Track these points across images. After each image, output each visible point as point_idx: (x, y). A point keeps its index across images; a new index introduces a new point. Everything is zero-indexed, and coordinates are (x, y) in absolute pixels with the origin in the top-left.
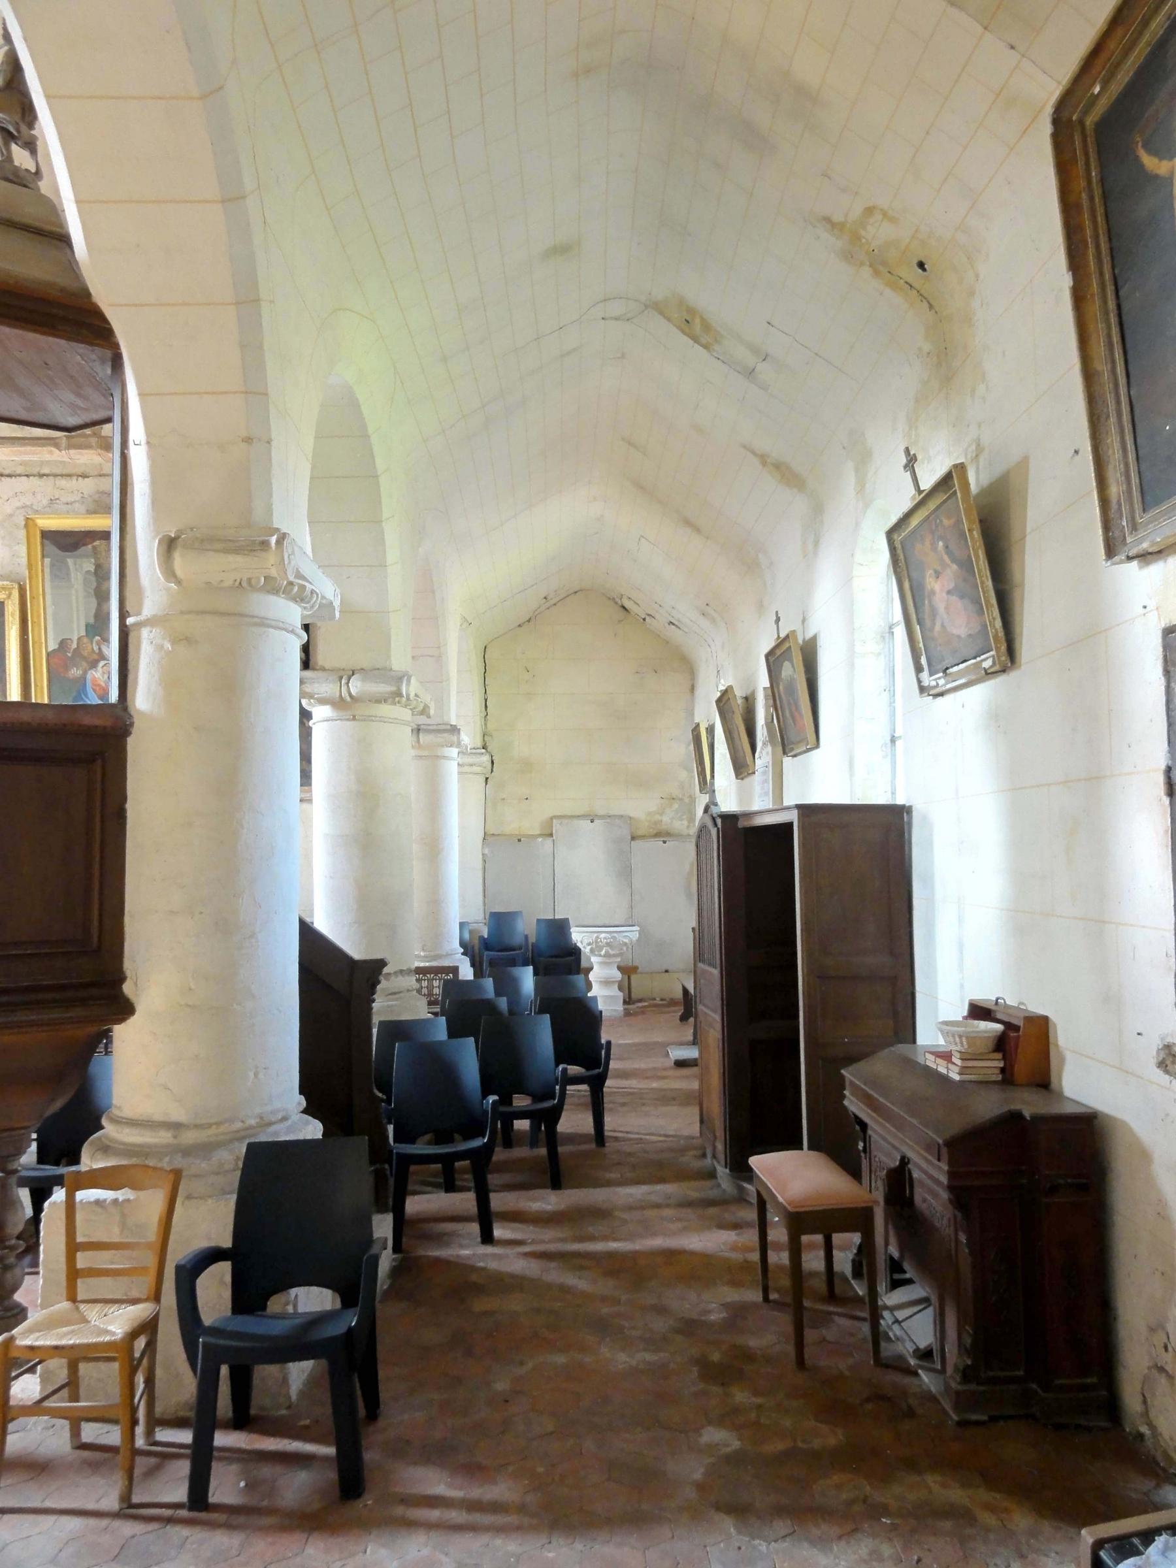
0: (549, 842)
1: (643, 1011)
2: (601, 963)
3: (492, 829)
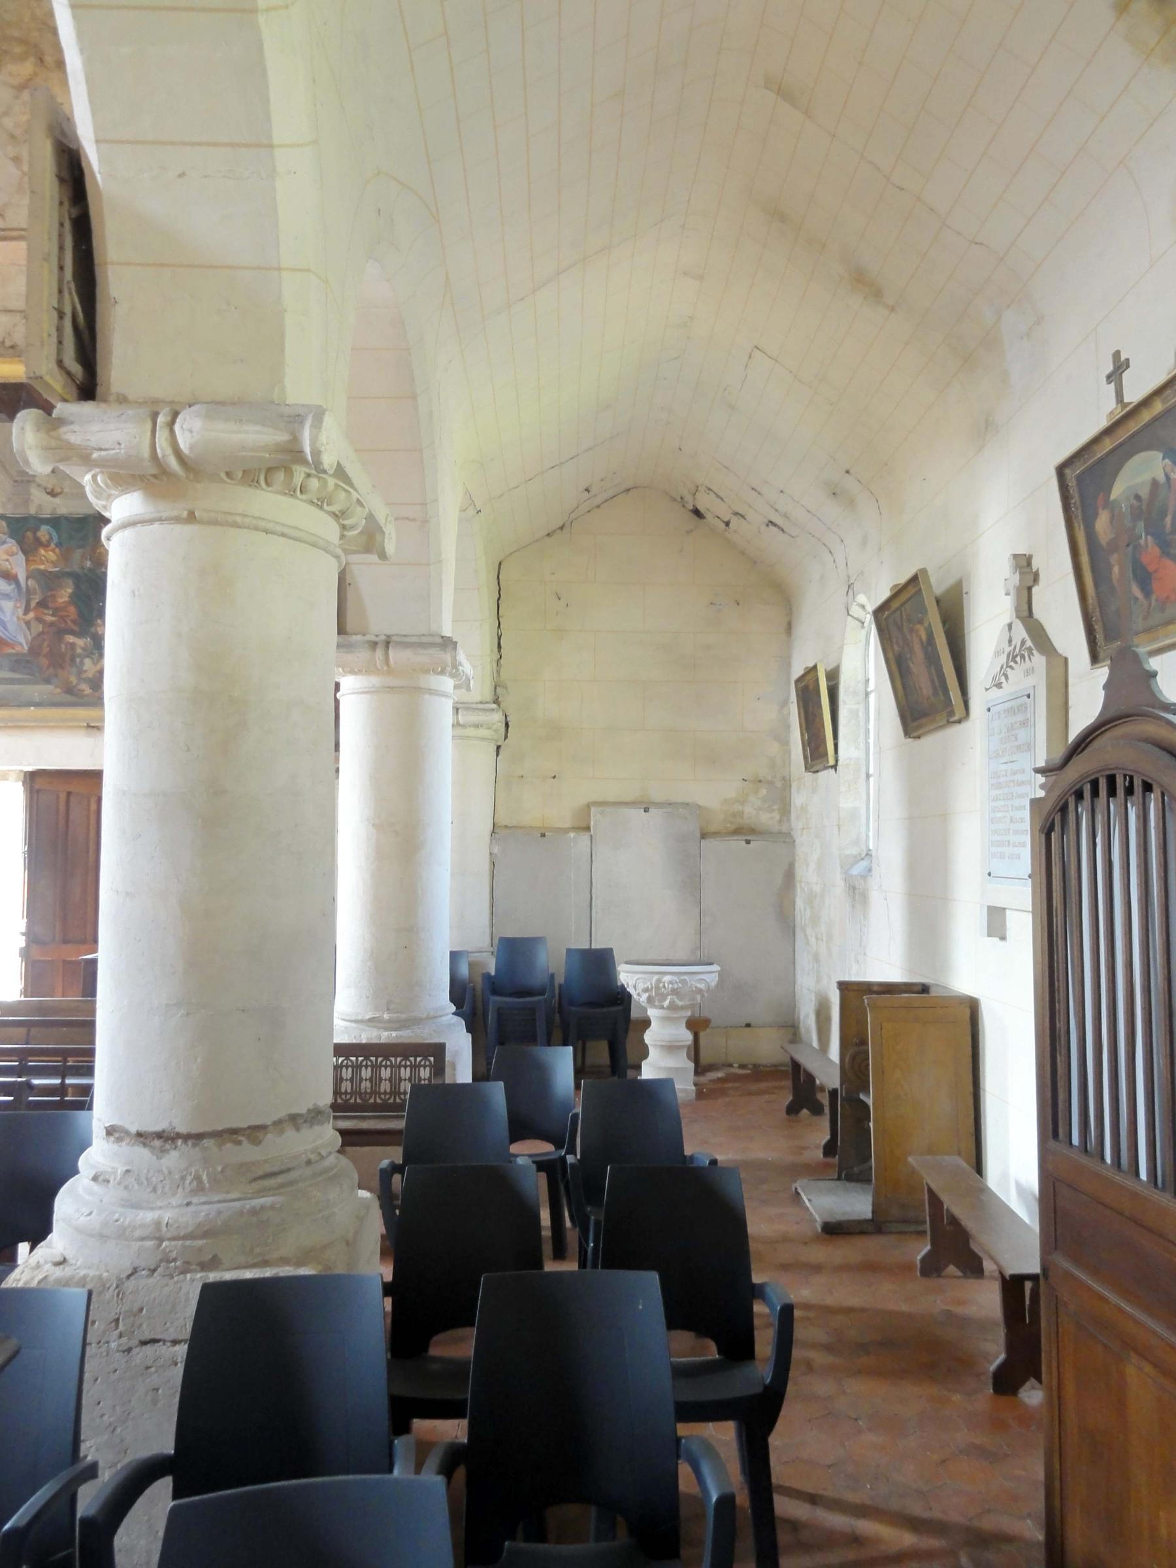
0: (584, 838)
2: (665, 1019)
3: (503, 819)
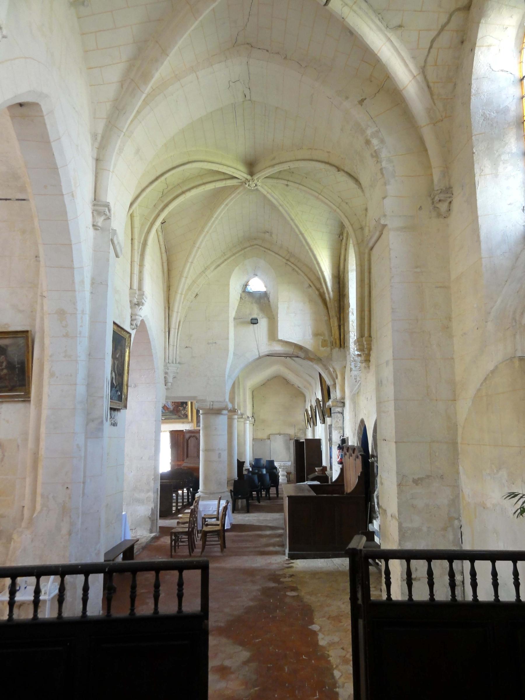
0: (269, 441)
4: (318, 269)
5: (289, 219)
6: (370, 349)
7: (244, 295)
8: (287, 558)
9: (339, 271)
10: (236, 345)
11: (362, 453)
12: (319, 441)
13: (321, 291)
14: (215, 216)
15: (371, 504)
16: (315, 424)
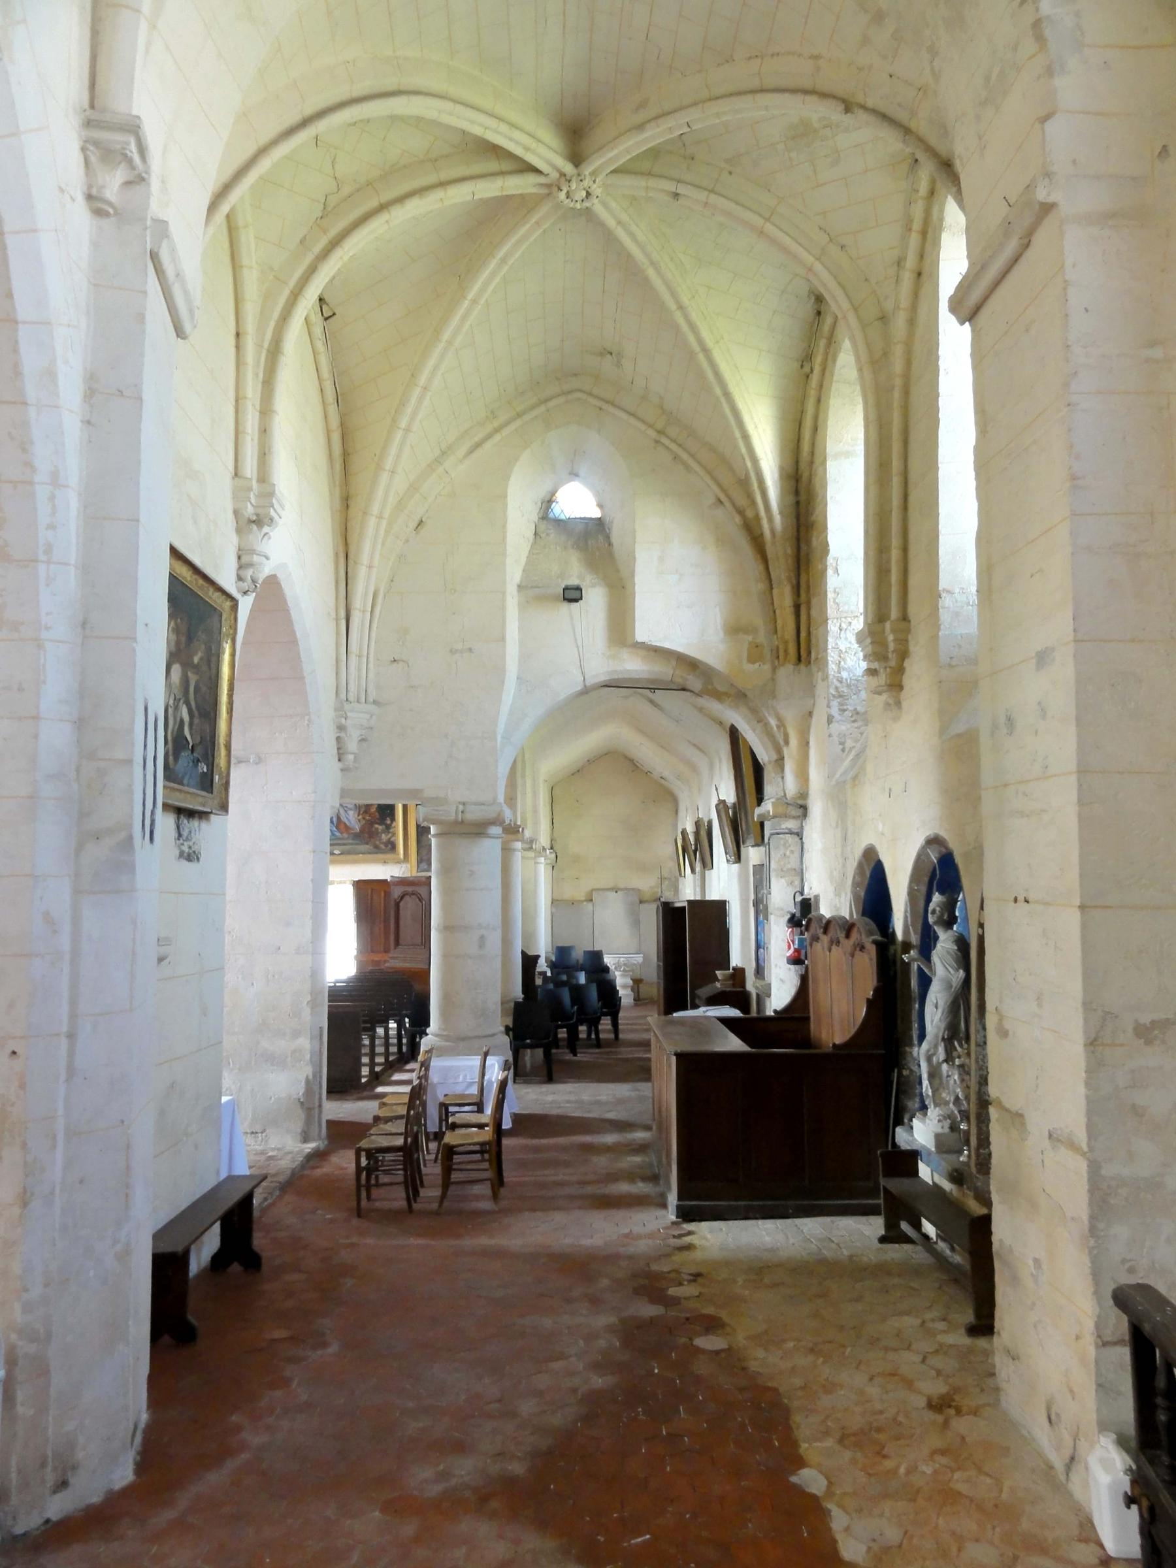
0: (590, 905)
1: (646, 1004)
2: (622, 976)
4: (744, 450)
5: (672, 306)
6: (903, 654)
7: (543, 526)
8: (673, 1218)
9: (797, 462)
10: (525, 657)
11: (878, 938)
12: (720, 908)
13: (750, 514)
14: (470, 296)
15: (900, 1075)
16: (707, 864)
